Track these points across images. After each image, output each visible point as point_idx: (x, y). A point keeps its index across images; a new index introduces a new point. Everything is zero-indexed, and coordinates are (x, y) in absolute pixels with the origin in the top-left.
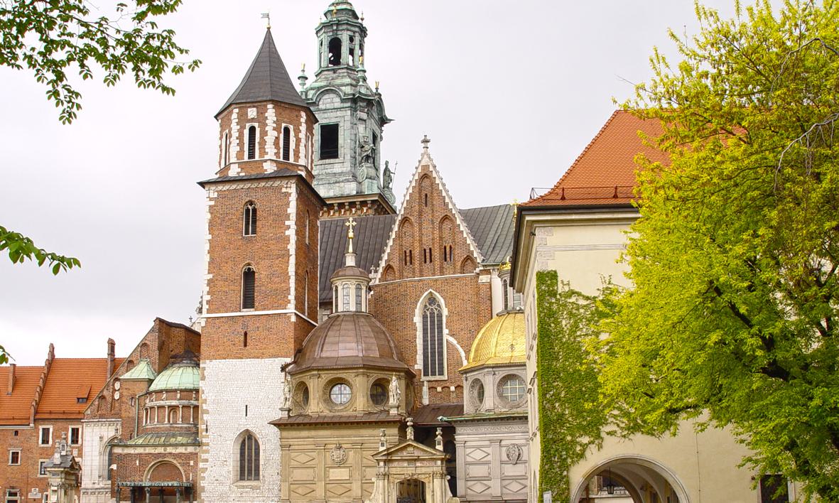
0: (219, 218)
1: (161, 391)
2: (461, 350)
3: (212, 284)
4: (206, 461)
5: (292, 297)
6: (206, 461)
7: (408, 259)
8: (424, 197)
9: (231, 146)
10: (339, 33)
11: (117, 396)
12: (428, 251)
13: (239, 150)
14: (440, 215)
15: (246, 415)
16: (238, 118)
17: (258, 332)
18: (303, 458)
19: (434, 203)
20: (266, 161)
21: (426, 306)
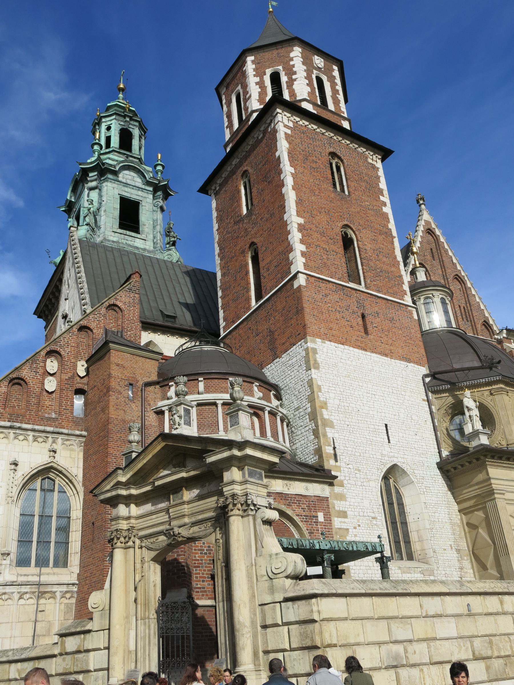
0: (300, 154)
4: (343, 514)
5: (406, 287)
6: (343, 514)
8: (430, 250)
9: (295, 82)
10: (130, 126)
11: (51, 384)
13: (310, 91)
15: (389, 442)
16: (302, 57)
17: (378, 320)
20: (345, 119)
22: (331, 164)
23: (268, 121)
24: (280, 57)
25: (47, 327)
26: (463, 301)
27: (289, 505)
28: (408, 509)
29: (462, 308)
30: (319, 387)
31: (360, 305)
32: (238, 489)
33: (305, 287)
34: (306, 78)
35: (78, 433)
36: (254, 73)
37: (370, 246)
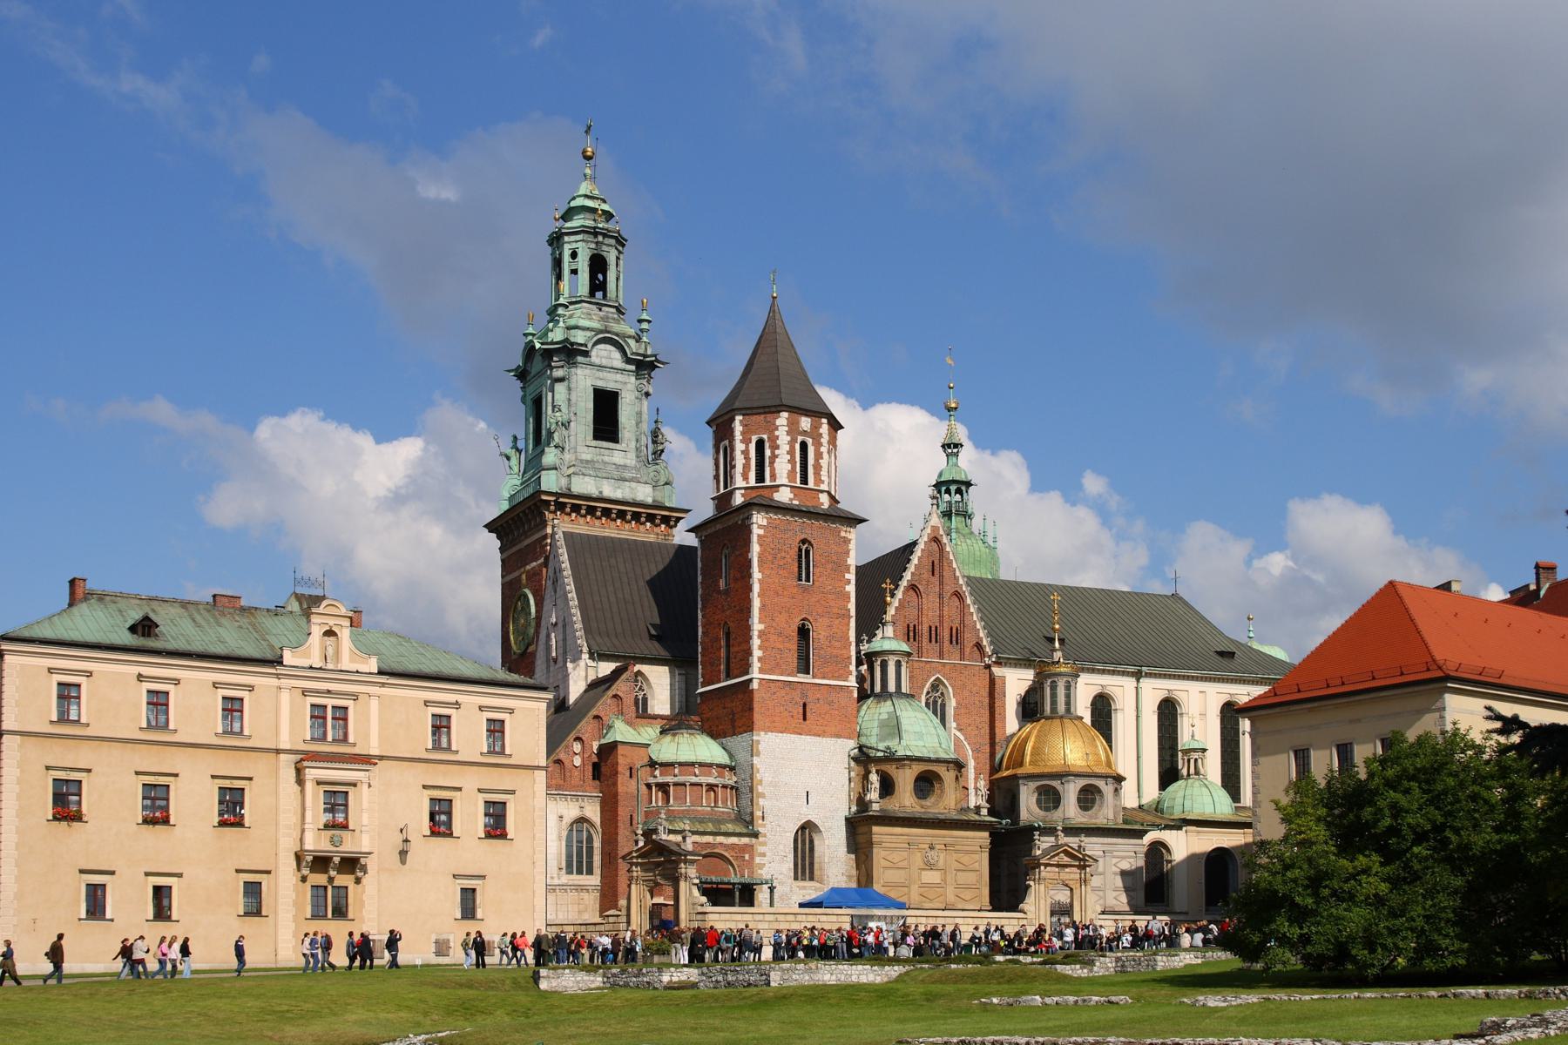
1: (693, 764)
2: (968, 748)
3: (764, 637)
4: (764, 855)
5: (853, 667)
6: (764, 855)
7: (911, 634)
9: (777, 460)
11: (577, 761)
12: (933, 629)
13: (790, 468)
14: (949, 589)
16: (788, 425)
17: (818, 705)
18: (896, 857)
19: (944, 574)
21: (928, 693)
22: (800, 550)
23: (746, 515)
24: (767, 422)
25: (506, 550)
26: (958, 621)
27: (727, 850)
28: (816, 848)
29: (954, 631)
30: (758, 770)
31: (804, 695)
32: (683, 871)
33: (758, 690)
34: (788, 453)
35: (596, 795)
36: (741, 437)
37: (823, 633)
